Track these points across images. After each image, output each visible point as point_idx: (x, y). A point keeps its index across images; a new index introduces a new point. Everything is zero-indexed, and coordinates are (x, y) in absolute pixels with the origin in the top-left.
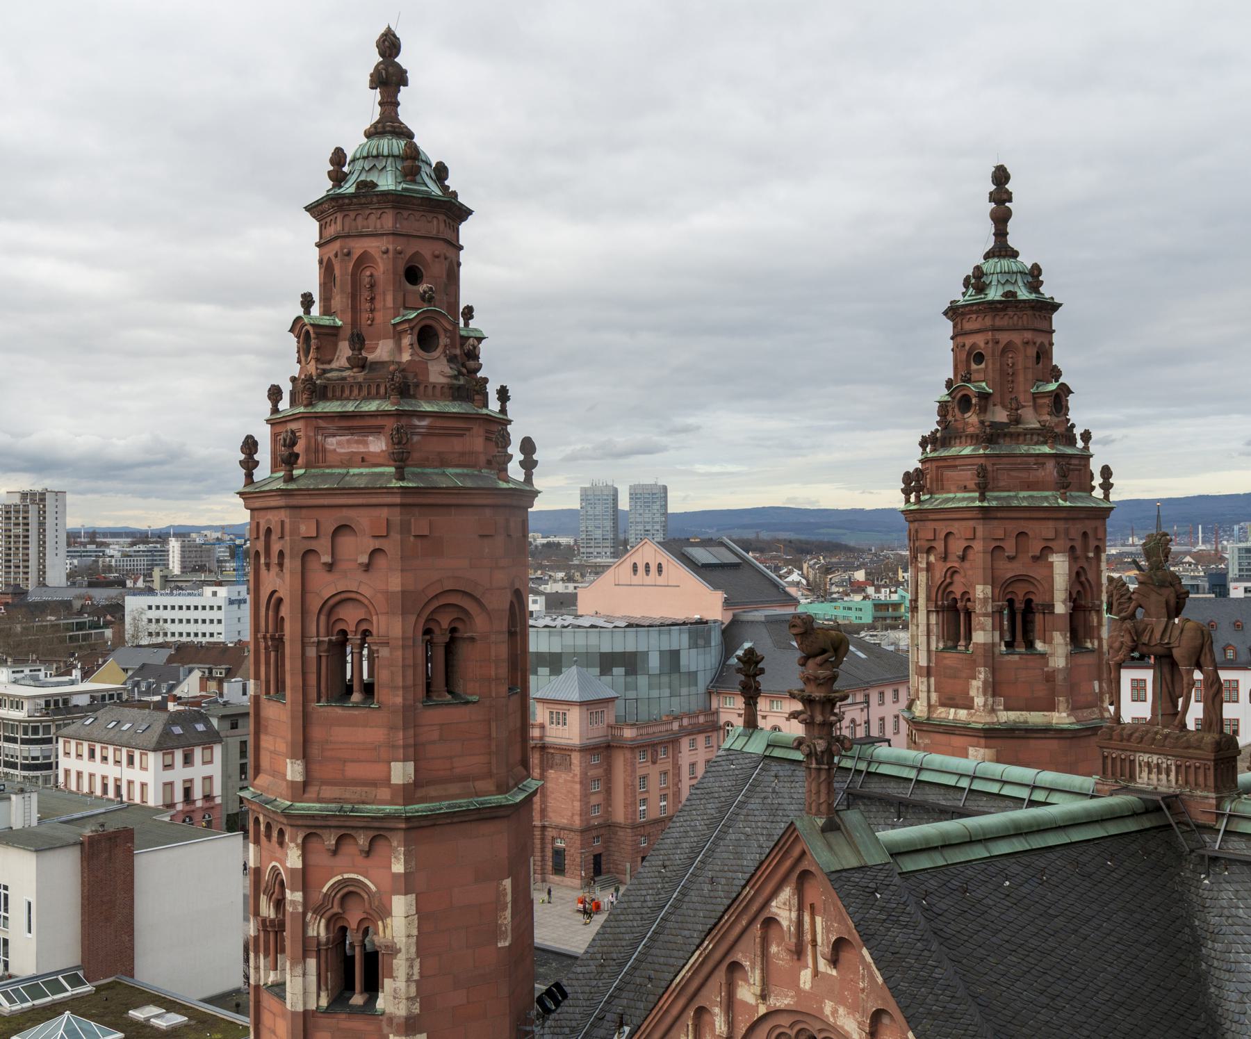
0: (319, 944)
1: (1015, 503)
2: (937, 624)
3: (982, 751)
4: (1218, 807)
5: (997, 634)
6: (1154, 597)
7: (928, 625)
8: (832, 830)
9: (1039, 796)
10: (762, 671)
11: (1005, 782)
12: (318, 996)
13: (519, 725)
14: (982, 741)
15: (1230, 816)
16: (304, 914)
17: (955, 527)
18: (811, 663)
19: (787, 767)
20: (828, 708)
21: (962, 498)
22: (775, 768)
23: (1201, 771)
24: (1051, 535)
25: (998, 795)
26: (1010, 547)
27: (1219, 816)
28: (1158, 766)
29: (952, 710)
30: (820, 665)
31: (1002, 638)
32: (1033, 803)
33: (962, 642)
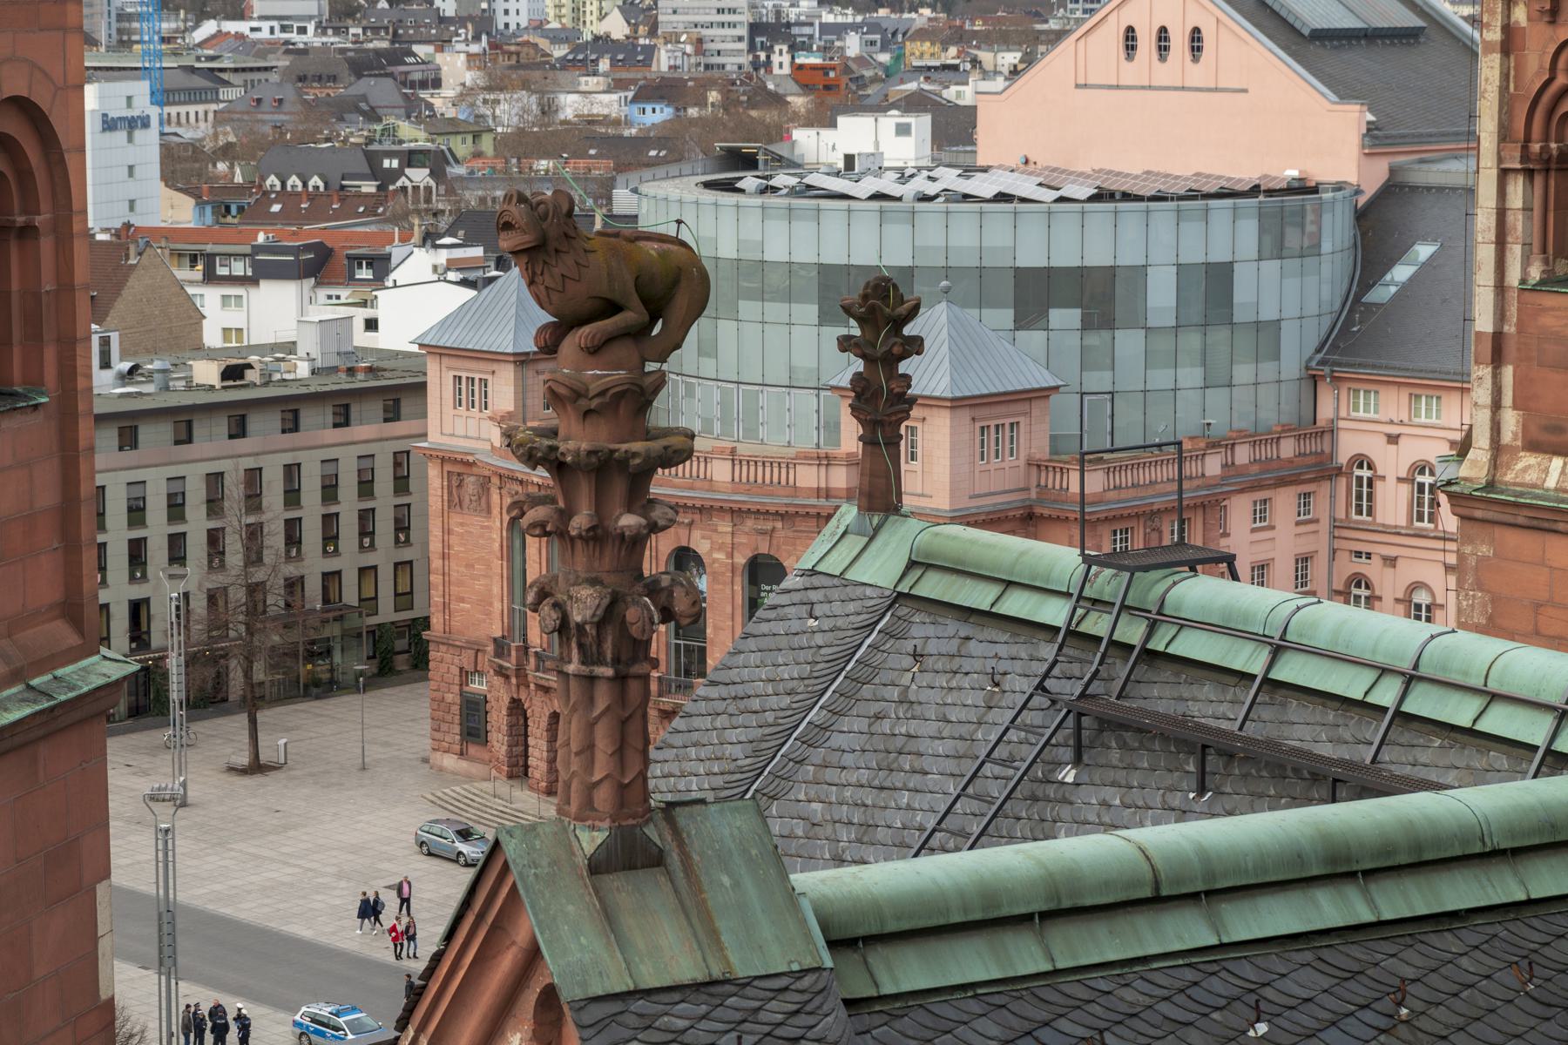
2: (1527, 209)
7: (1501, 213)
8: (630, 866)
10: (915, 346)
11: (1494, 697)
13: (47, 497)
18: (572, 343)
19: (952, 626)
20: (618, 488)
22: (921, 629)
25: (1470, 732)
30: (594, 350)
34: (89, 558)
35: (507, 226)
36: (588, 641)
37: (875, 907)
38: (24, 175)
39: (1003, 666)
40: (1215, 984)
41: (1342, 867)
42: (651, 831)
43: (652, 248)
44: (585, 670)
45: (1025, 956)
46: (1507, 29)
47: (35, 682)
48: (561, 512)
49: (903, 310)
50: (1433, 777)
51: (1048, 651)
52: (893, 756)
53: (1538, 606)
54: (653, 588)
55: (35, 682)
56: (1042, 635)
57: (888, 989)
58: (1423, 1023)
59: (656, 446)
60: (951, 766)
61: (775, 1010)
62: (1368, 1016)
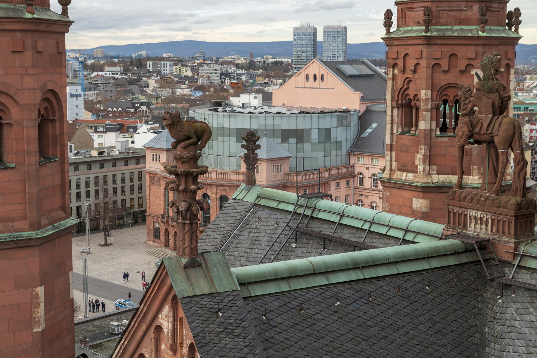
1: (449, 34)
2: (398, 116)
3: (421, 201)
4: (516, 249)
5: (434, 123)
6: (485, 100)
7: (392, 117)
8: (194, 267)
9: (410, 237)
10: (259, 147)
13: (58, 182)
14: (421, 195)
15: (522, 255)
17: (411, 50)
19: (267, 211)
21: (417, 30)
22: (260, 212)
23: (507, 224)
24: (473, 56)
25: (385, 235)
26: (444, 64)
27: (515, 255)
28: (481, 219)
29: (405, 174)
30: (185, 148)
31: (437, 126)
32: (405, 242)
33: (413, 129)
34: (67, 196)
35: (165, 119)
36: (184, 215)
37: (249, 276)
38: (53, 107)
39: (279, 220)
40: (328, 293)
41: (356, 266)
42: (198, 259)
43: (198, 124)
44: (183, 221)
45: (284, 287)
46: (393, 75)
47: (55, 225)
48: (177, 185)
49: (256, 139)
50: (377, 245)
51: (289, 217)
52: (254, 241)
53: (400, 206)
54: (199, 203)
55: (55, 225)
56: (288, 213)
57: (253, 295)
58: (375, 302)
59: (199, 170)
60: (267, 243)
61: (227, 300)
62: (362, 300)
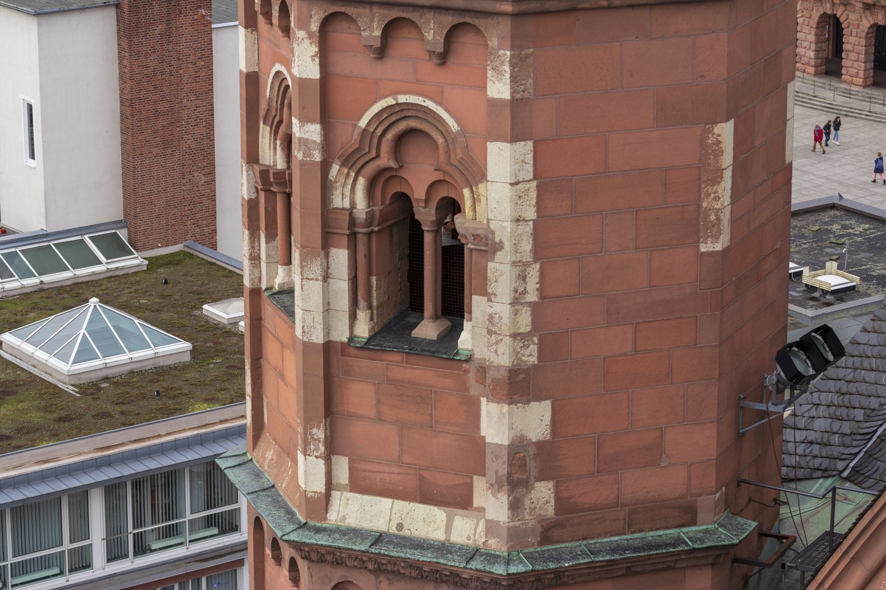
0: (352, 222)
12: (353, 317)
16: (325, 166)
